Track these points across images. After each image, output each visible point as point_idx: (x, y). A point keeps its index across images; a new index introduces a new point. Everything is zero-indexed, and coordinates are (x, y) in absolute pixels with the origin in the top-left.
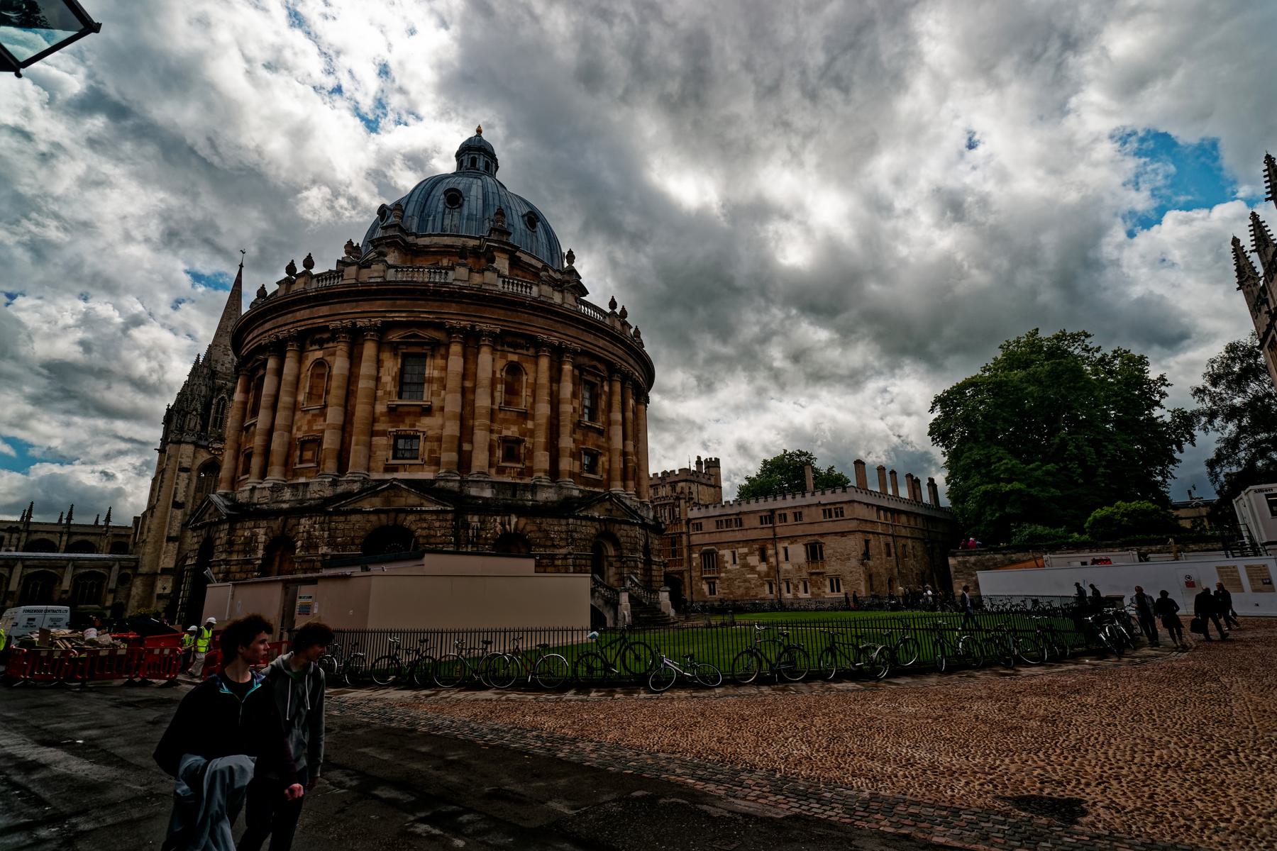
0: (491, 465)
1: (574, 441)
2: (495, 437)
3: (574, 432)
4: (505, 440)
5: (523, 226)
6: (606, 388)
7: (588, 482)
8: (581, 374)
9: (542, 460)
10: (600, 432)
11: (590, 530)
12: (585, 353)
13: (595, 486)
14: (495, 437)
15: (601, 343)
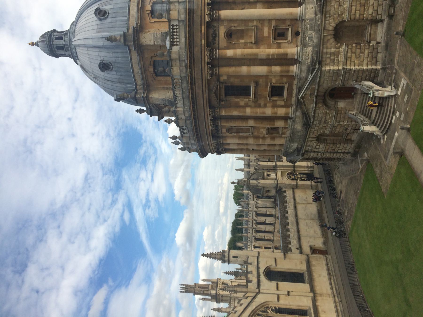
0: (281, 137)
1: (265, 106)
2: (266, 136)
3: (259, 106)
4: (268, 133)
5: (114, 73)
6: (224, 78)
7: (290, 95)
8: (223, 101)
9: (280, 124)
10: (257, 84)
11: (321, 110)
12: (211, 106)
13: (292, 89)
14: (266, 136)
15: (199, 91)
